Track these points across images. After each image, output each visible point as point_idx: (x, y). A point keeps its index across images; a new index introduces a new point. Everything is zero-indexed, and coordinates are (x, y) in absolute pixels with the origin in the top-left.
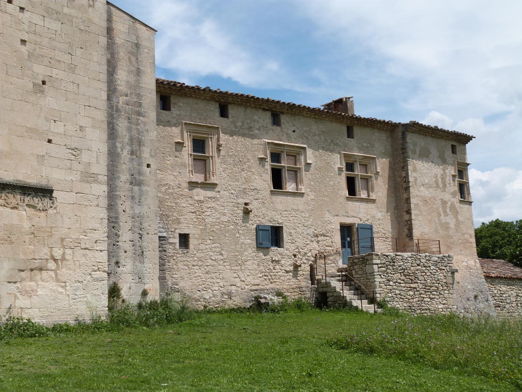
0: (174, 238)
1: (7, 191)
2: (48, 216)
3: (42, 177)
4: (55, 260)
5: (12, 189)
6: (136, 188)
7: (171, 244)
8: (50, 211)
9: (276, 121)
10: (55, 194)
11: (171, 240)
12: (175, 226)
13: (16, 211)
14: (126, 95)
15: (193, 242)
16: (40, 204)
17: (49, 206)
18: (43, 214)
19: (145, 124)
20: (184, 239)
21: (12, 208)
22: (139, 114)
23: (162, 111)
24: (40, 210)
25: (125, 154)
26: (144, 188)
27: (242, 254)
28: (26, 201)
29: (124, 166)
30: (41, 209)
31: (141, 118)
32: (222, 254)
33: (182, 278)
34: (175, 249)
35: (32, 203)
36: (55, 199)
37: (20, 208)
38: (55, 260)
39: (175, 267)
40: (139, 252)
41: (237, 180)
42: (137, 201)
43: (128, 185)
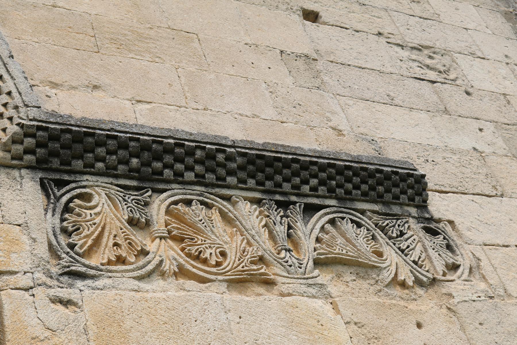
1: (177, 193)
2: (461, 309)
3: (340, 133)
5: (200, 180)
8: (458, 287)
10: (438, 205)
13: (268, 299)
16: (391, 256)
17: (440, 268)
18: (426, 304)
21: (239, 282)
24: (403, 285)
28: (308, 244)
30: (405, 274)
35: (340, 248)
36: (449, 228)
37: (284, 284)
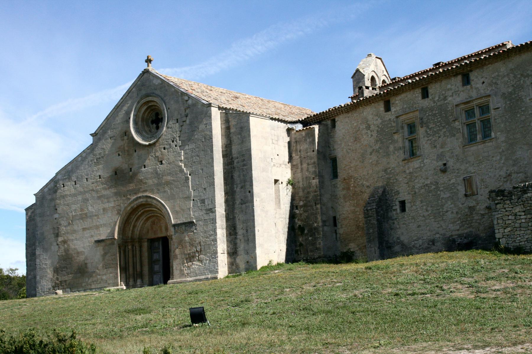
0: (396, 205)
4: (198, 252)
6: (244, 206)
7: (394, 210)
9: (466, 81)
11: (394, 208)
12: (396, 197)
14: (238, 158)
15: (408, 205)
19: (246, 169)
20: (403, 204)
22: (244, 165)
23: (387, 113)
25: (238, 190)
26: (247, 204)
27: (442, 206)
29: (238, 196)
31: (245, 167)
32: (427, 210)
33: (402, 234)
34: (397, 214)
38: (198, 252)
39: (398, 227)
40: (246, 239)
41: (435, 147)
42: (244, 213)
43: (240, 206)
